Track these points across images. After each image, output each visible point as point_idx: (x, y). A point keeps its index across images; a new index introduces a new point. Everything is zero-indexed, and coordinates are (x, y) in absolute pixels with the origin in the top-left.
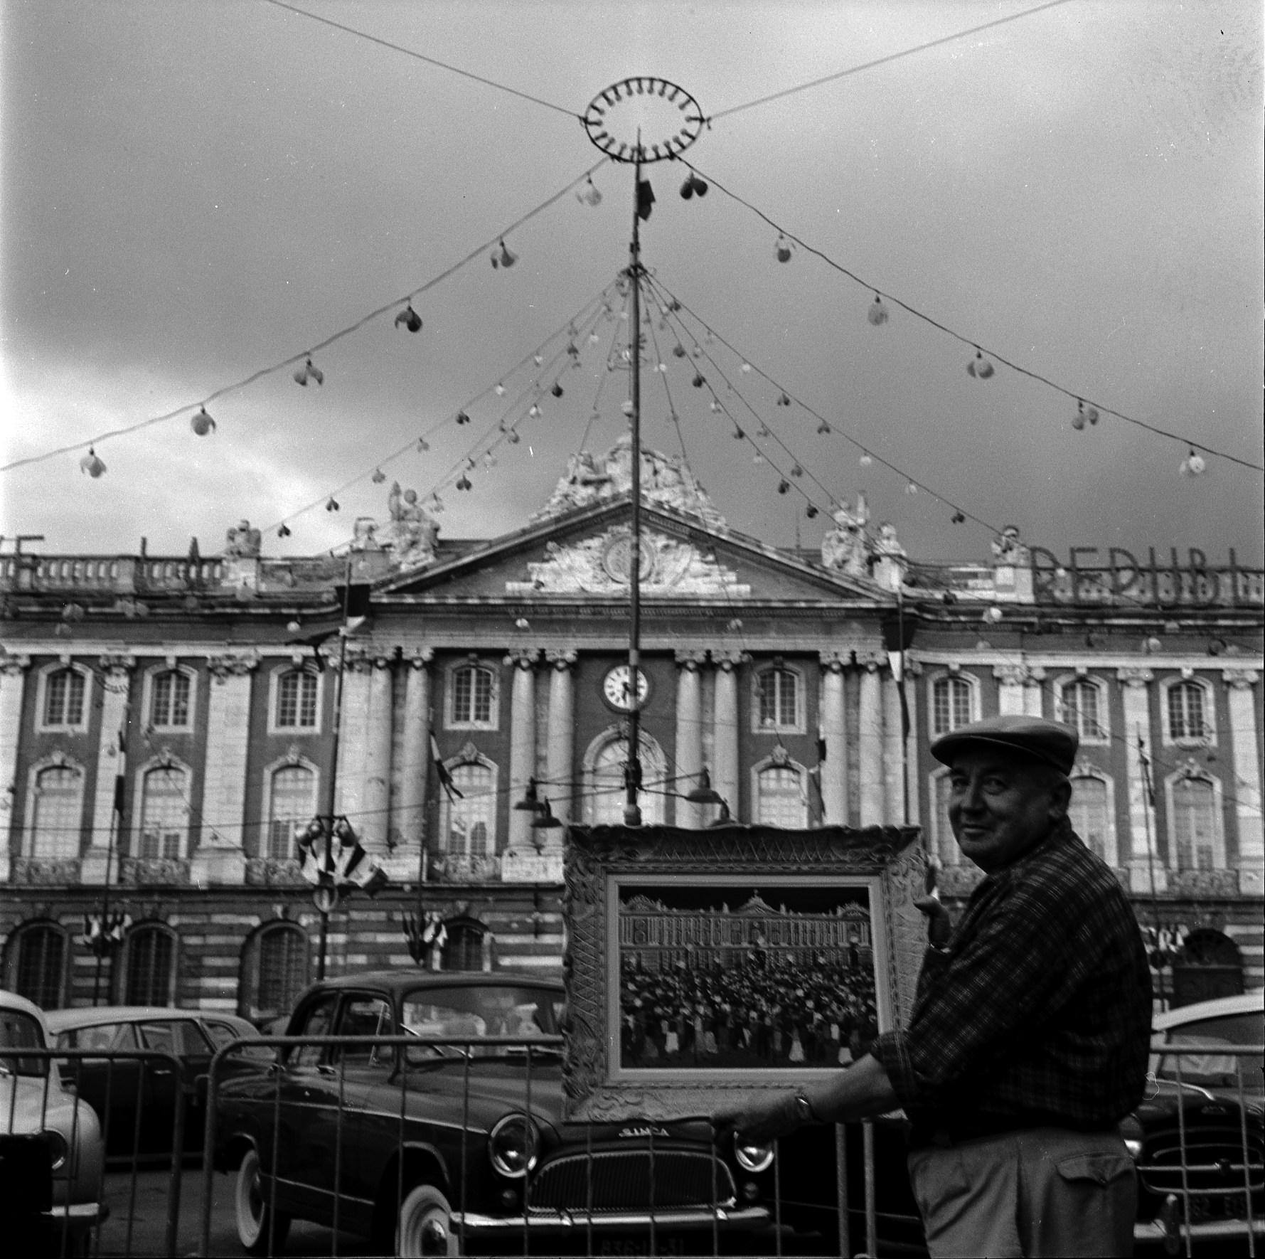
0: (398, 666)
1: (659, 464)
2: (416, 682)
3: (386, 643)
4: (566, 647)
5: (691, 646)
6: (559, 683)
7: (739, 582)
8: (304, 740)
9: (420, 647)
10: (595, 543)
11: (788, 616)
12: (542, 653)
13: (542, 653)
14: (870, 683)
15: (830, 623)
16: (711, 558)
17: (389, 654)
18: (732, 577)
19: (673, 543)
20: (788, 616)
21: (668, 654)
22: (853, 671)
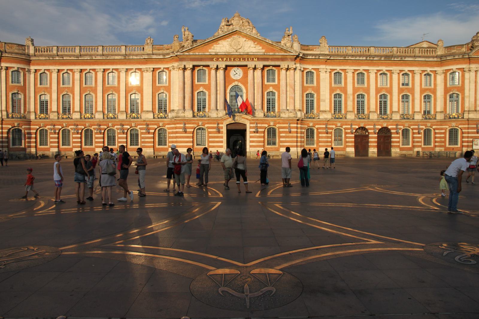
1: (244, 21)
2: (188, 73)
3: (182, 64)
5: (251, 64)
6: (221, 73)
7: (263, 49)
8: (164, 87)
10: (229, 40)
12: (217, 66)
13: (217, 66)
15: (283, 59)
16: (256, 43)
17: (183, 67)
18: (261, 48)
19: (247, 40)
21: (246, 66)
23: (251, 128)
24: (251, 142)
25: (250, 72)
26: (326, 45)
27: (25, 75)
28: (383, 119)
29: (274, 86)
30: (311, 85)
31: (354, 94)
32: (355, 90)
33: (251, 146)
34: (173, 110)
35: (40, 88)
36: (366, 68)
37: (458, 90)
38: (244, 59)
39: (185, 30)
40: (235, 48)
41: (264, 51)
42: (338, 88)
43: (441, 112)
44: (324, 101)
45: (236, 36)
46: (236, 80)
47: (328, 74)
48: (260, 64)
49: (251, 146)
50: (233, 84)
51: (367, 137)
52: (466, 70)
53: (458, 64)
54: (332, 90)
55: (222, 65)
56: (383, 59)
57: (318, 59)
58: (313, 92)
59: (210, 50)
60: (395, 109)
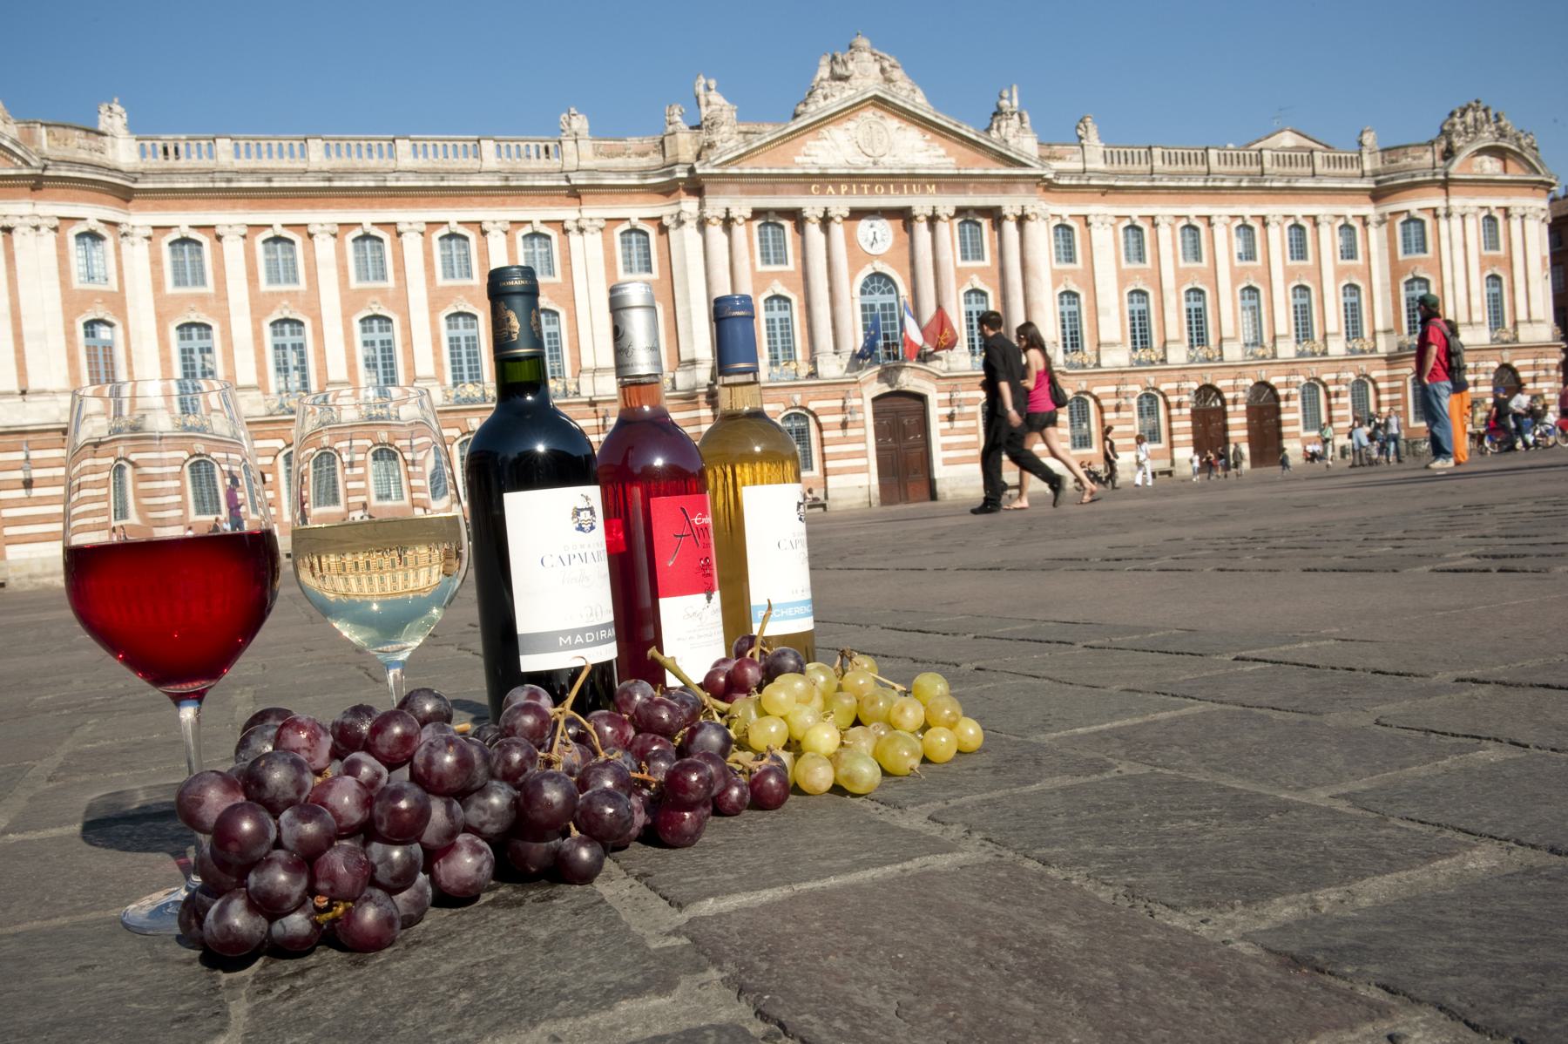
0: (728, 222)
4: (840, 205)
7: (948, 155)
9: (742, 207)
10: (851, 125)
11: (983, 182)
12: (826, 212)
13: (826, 212)
14: (1030, 226)
18: (942, 152)
20: (983, 182)
22: (1022, 220)
23: (941, 404)
24: (946, 447)
25: (922, 230)
26: (1097, 142)
27: (118, 248)
28: (1257, 358)
29: (981, 272)
30: (1070, 266)
31: (1178, 289)
32: (1180, 276)
33: (947, 462)
34: (693, 362)
35: (174, 297)
36: (1205, 211)
37: (1426, 270)
38: (899, 188)
39: (708, 88)
40: (869, 151)
41: (953, 160)
42: (1137, 271)
43: (1387, 332)
44: (1108, 313)
45: (870, 114)
46: (877, 256)
47: (1110, 232)
48: (946, 204)
49: (947, 462)
50: (868, 270)
51: (1223, 414)
52: (1441, 212)
53: (1421, 197)
54: (1123, 278)
55: (840, 205)
56: (1244, 184)
57: (1081, 188)
58: (1074, 289)
59: (798, 159)
60: (1227, 331)
